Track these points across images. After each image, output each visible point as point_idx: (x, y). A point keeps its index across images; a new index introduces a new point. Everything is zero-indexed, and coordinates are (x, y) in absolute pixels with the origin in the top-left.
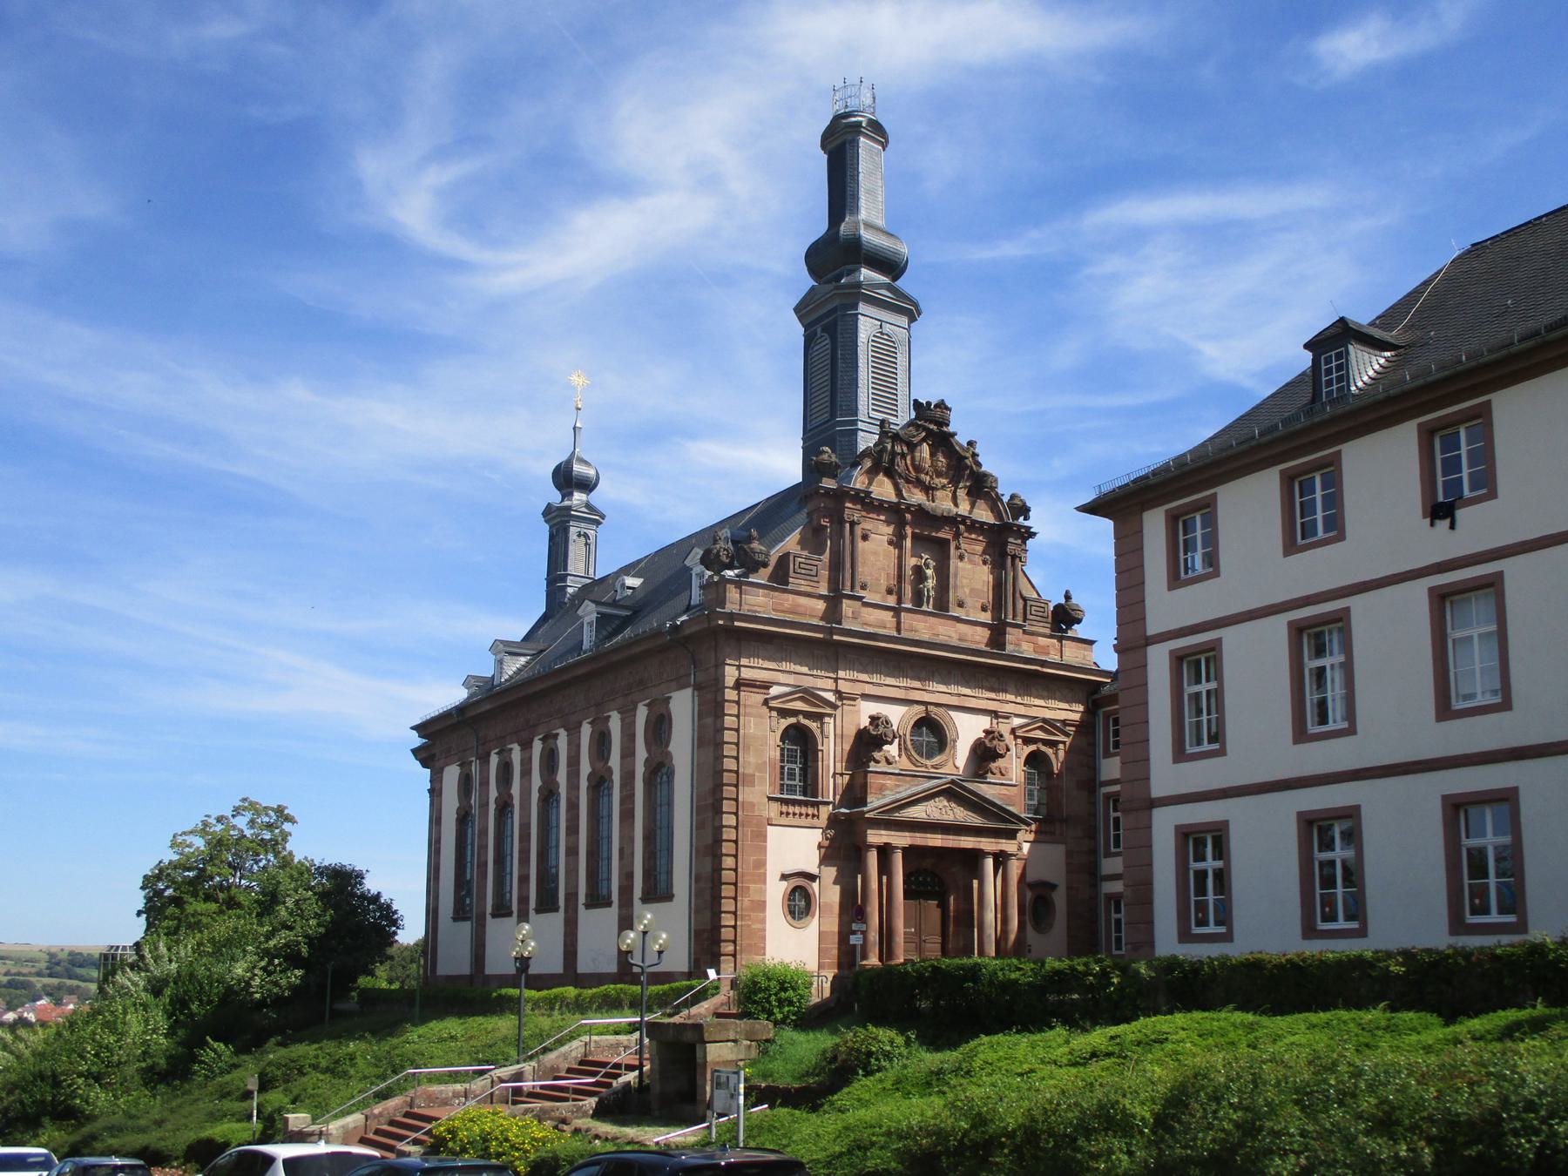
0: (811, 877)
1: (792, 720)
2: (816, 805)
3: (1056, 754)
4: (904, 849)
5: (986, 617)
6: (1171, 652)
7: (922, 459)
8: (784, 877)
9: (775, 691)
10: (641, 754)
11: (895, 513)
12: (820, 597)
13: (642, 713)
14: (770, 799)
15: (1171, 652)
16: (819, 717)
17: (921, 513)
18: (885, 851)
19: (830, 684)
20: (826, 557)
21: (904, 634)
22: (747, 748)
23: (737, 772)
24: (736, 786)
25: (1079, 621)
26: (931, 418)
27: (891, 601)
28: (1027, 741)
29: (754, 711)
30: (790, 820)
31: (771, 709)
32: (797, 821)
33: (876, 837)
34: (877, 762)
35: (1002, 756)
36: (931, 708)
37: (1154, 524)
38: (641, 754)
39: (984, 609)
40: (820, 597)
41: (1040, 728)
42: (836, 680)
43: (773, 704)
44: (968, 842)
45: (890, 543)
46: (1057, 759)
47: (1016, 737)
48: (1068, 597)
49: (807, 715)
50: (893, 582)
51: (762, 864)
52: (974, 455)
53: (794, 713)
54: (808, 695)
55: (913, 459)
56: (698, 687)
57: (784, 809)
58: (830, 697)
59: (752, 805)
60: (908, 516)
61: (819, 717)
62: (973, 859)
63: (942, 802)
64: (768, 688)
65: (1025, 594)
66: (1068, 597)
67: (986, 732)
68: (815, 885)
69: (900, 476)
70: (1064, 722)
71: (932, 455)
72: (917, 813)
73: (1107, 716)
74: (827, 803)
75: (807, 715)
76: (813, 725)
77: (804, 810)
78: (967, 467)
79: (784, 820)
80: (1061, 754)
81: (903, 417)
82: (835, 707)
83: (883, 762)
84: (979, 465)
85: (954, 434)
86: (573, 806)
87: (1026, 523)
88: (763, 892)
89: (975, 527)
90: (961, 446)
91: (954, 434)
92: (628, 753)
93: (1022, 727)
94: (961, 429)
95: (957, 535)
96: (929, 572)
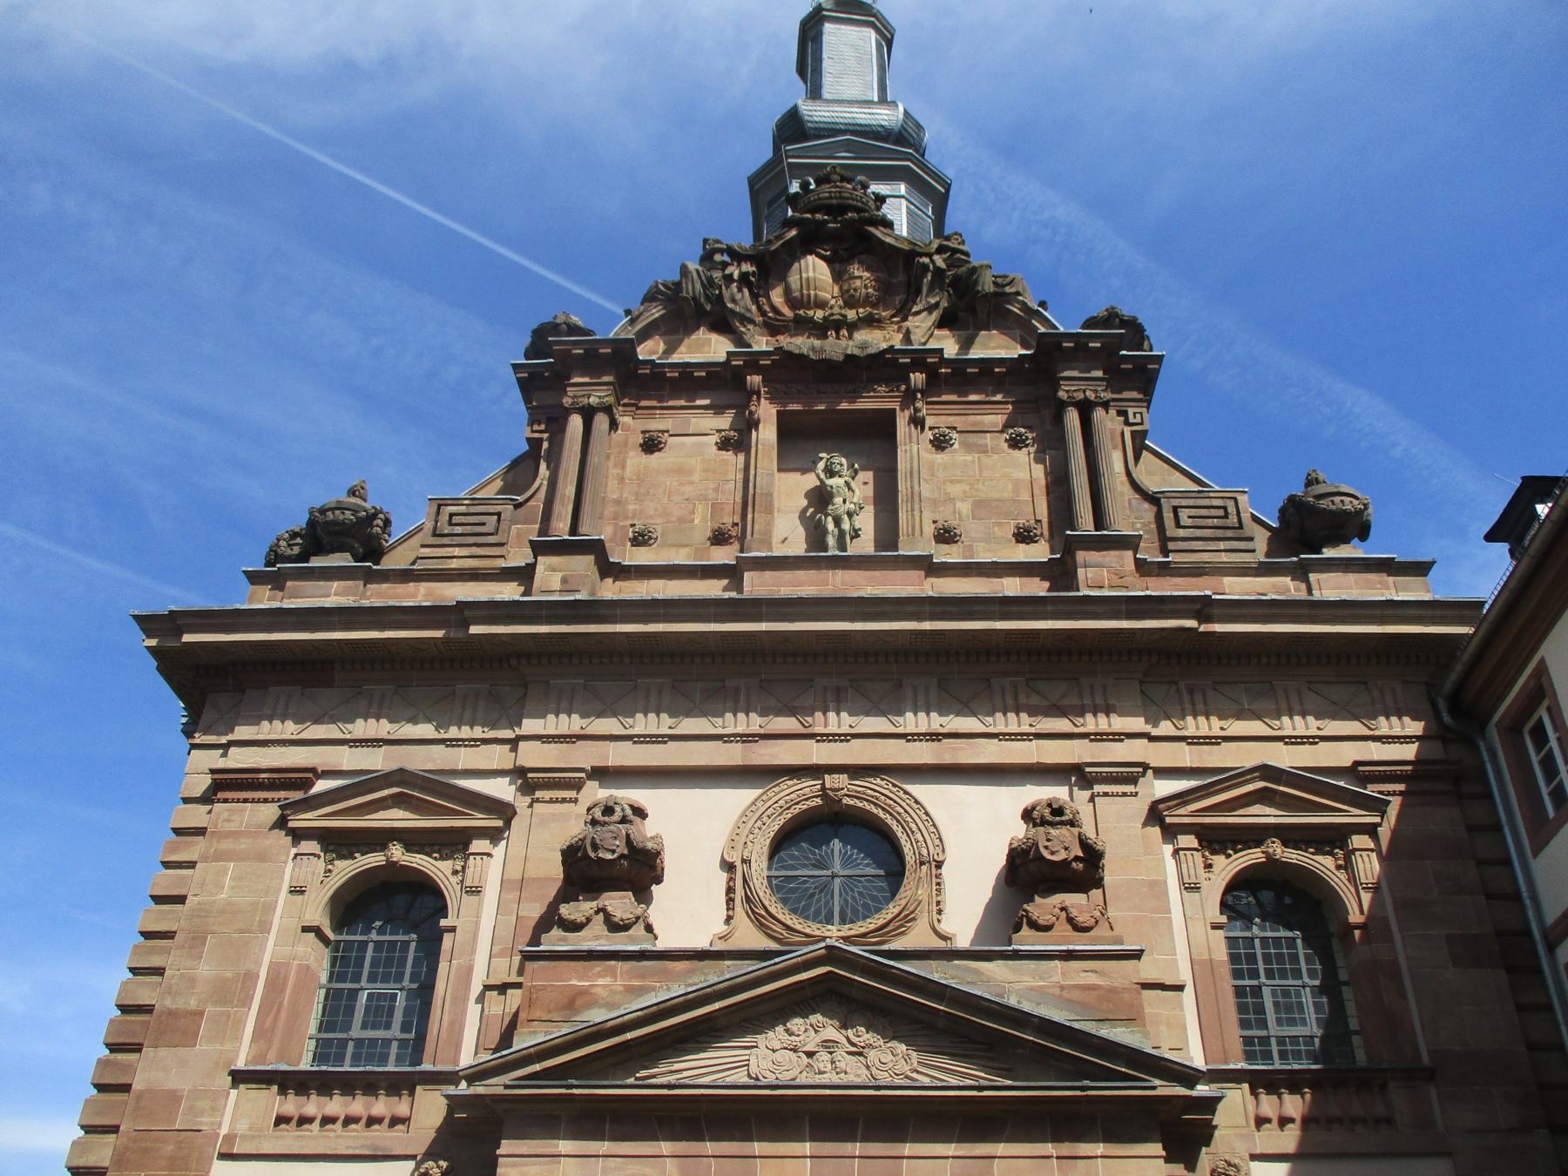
2: (401, 1085)
3: (1347, 866)
29: (244, 844)
30: (313, 1139)
31: (298, 835)
32: (337, 1139)
34: (574, 927)
36: (830, 781)
39: (1024, 536)
46: (1357, 879)
48: (1311, 482)
53: (377, 839)
58: (502, 789)
65: (1152, 486)
69: (745, 320)
70: (1355, 771)
71: (838, 277)
75: (415, 840)
76: (439, 869)
78: (925, 268)
79: (290, 1140)
80: (1369, 866)
82: (505, 811)
89: (985, 375)
93: (1182, 798)
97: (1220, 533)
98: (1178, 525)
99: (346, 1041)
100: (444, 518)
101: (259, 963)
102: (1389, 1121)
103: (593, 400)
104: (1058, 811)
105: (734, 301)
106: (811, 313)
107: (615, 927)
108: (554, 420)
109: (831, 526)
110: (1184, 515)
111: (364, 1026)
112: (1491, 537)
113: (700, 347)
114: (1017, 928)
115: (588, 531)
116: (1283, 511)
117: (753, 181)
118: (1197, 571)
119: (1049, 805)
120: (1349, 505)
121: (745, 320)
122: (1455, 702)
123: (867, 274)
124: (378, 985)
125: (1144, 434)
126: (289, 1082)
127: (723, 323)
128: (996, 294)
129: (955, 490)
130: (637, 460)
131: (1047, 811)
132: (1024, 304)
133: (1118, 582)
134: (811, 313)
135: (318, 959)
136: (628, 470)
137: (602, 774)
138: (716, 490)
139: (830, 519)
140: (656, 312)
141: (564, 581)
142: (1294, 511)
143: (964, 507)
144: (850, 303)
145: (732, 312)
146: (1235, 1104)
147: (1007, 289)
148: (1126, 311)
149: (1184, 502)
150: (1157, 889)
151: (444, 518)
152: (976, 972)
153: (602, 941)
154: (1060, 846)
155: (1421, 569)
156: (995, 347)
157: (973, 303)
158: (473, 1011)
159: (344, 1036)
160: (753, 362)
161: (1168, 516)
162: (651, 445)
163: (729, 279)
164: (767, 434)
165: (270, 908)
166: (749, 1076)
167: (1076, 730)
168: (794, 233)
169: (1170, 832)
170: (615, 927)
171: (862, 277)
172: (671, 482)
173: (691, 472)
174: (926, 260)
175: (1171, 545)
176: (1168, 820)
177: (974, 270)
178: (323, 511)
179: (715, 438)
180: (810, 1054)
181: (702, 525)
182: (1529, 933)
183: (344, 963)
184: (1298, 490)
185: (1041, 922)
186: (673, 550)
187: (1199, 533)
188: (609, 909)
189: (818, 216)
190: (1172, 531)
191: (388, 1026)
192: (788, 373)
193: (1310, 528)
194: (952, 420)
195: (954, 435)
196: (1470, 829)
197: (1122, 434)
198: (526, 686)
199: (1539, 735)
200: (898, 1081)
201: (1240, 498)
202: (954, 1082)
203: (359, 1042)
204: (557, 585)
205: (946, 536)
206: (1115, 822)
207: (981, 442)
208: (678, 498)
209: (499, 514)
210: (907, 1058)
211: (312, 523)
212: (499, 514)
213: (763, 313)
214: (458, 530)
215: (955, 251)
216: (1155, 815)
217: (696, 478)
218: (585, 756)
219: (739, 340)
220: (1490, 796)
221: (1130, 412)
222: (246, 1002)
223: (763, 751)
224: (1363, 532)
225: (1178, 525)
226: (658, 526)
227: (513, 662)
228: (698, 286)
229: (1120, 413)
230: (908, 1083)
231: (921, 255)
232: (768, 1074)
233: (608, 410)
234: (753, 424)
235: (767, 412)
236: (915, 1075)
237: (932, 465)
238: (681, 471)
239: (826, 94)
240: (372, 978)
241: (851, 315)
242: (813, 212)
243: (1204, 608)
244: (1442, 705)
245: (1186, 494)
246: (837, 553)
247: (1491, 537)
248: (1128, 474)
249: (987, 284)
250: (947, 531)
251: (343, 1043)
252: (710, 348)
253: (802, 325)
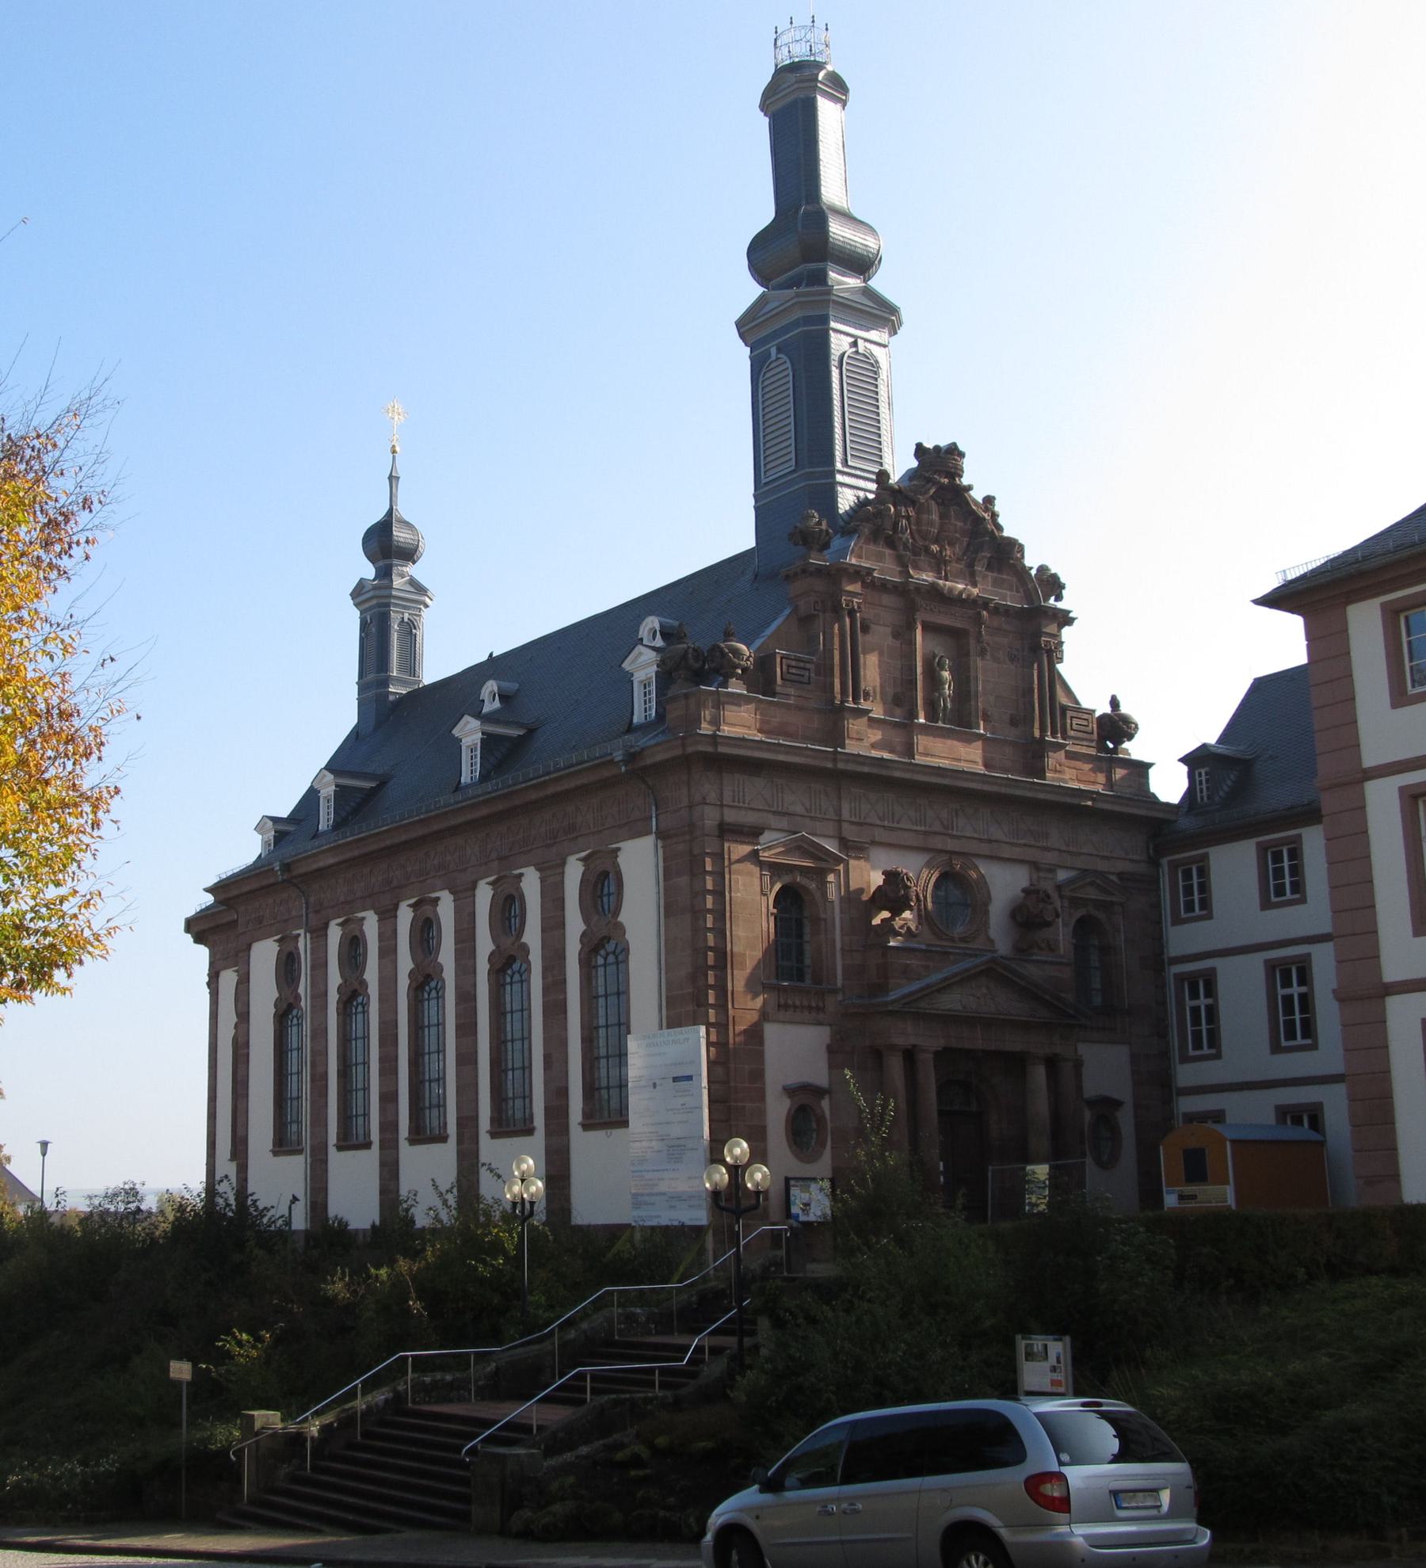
0: (818, 1092)
1: (787, 879)
4: (937, 1053)
6: (1402, 790)
7: (931, 523)
8: (790, 1091)
9: (766, 837)
10: (575, 925)
13: (574, 872)
15: (1402, 790)
16: (820, 874)
17: (935, 594)
18: (910, 1056)
21: (919, 759)
25: (1130, 737)
26: (939, 465)
31: (761, 865)
33: (905, 1034)
35: (1048, 924)
37: (1365, 622)
38: (575, 925)
41: (1092, 883)
43: (765, 856)
44: (1013, 1043)
47: (1061, 897)
48: (1114, 703)
51: (758, 1075)
52: (994, 516)
53: (791, 869)
55: (919, 522)
56: (661, 835)
58: (831, 846)
62: (1016, 1063)
66: (1114, 703)
67: (1024, 890)
68: (825, 1104)
71: (941, 517)
72: (952, 1001)
73: (1174, 867)
74: (835, 991)
81: (900, 463)
82: (839, 860)
84: (1000, 528)
85: (970, 488)
86: (466, 998)
87: (1060, 605)
88: (762, 1113)
90: (974, 501)
91: (970, 488)
92: (553, 925)
94: (978, 479)
96: (946, 674)
110: (1075, 721)
112: (1181, 760)
121: (906, 548)
164: (919, 631)
199: (1188, 875)
234: (911, 628)
247: (1181, 760)
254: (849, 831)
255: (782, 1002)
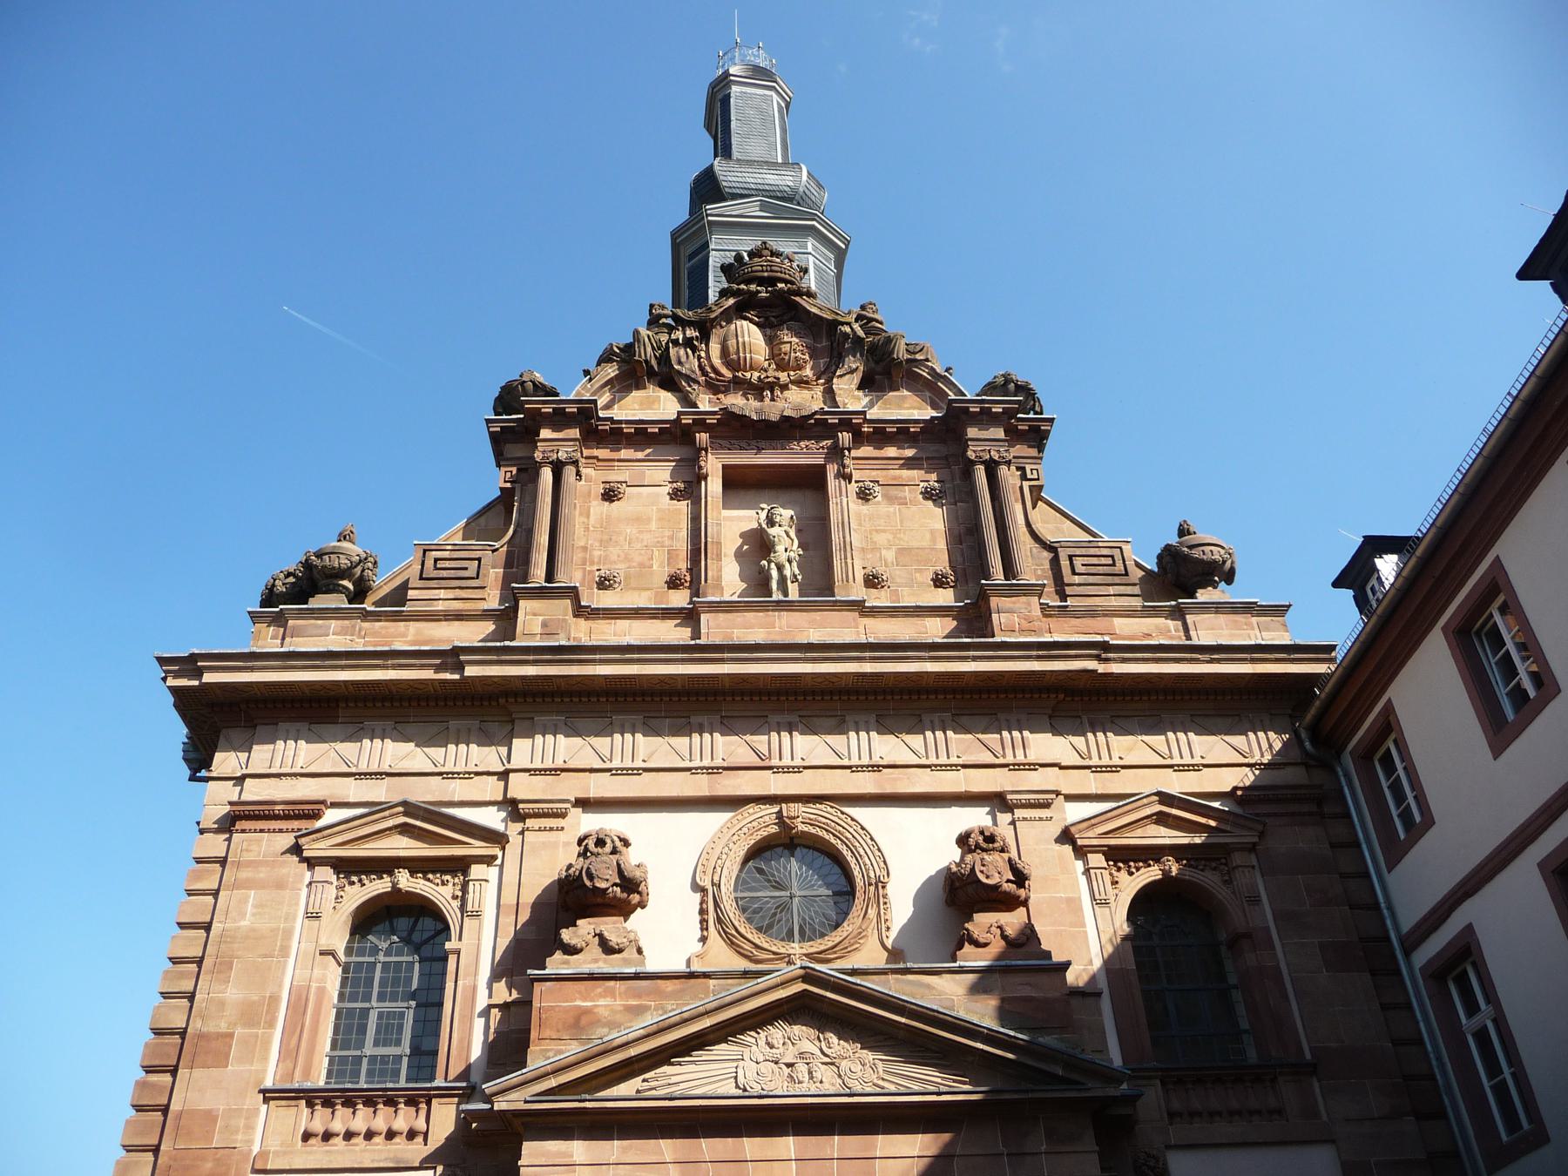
1: (381, 886)
5: (946, 597)
9: (331, 816)
11: (675, 438)
12: (485, 615)
14: (268, 1095)
19: (491, 789)
20: (502, 544)
22: (224, 966)
23: (183, 1033)
24: (174, 1072)
27: (680, 599)
28: (1122, 856)
31: (312, 863)
34: (571, 950)
39: (939, 582)
40: (485, 615)
42: (504, 775)
43: (314, 849)
45: (675, 495)
48: (1183, 531)
49: (418, 866)
50: (683, 565)
53: (384, 866)
54: (424, 818)
57: (320, 1119)
58: (492, 818)
59: (210, 1117)
60: (703, 438)
61: (459, 866)
63: (800, 1039)
64: (316, 816)
65: (1050, 537)
71: (771, 341)
75: (418, 866)
76: (440, 892)
77: (381, 1121)
82: (498, 839)
83: (595, 950)
89: (899, 433)
95: (836, 453)
97: (1109, 579)
98: (1074, 573)
99: (360, 1058)
100: (429, 563)
101: (280, 986)
102: (1279, 1112)
103: (562, 456)
104: (990, 839)
105: (680, 363)
106: (748, 375)
107: (607, 948)
108: (527, 473)
109: (774, 573)
110: (1078, 562)
111: (376, 1044)
112: (1337, 584)
113: (650, 403)
114: (960, 947)
115: (562, 580)
116: (1160, 557)
117: (675, 235)
118: (1092, 613)
119: (982, 833)
120: (1217, 555)
122: (1314, 730)
123: (795, 340)
124: (387, 1004)
125: (1040, 488)
126: (310, 1097)
127: (669, 380)
128: (908, 361)
129: (881, 539)
130: (599, 508)
131: (981, 838)
132: (933, 369)
133: (1025, 625)
134: (748, 375)
135: (332, 978)
136: (592, 520)
137: (585, 804)
138: (671, 538)
139: (773, 565)
140: (611, 371)
141: (544, 625)
142: (1169, 555)
143: (890, 555)
144: (782, 366)
145: (679, 372)
146: (1152, 1099)
147: (919, 357)
148: (1021, 377)
149: (1078, 552)
150: (1073, 904)
151: (429, 563)
152: (929, 986)
153: (601, 964)
154: (994, 871)
155: (1280, 610)
156: (908, 407)
157: (886, 368)
158: (479, 1024)
159: (358, 1053)
160: (700, 424)
161: (1065, 563)
162: (610, 495)
163: (676, 343)
164: (714, 486)
165: (288, 934)
166: (737, 1087)
167: (997, 761)
168: (731, 301)
169: (1081, 852)
170: (607, 948)
171: (792, 342)
172: (630, 530)
173: (649, 520)
174: (848, 329)
175: (1068, 590)
176: (1080, 842)
177: (889, 340)
178: (319, 555)
179: (668, 489)
180: (789, 1065)
181: (661, 572)
182: (1388, 939)
183: (355, 981)
184: (1173, 540)
185: (982, 940)
186: (636, 593)
187: (1091, 579)
188: (606, 934)
189: (753, 287)
190: (1067, 577)
191: (398, 1043)
192: (734, 429)
193: (1182, 574)
194: (874, 474)
195: (877, 488)
196: (1332, 846)
197: (1021, 488)
198: (513, 722)
199: (1387, 761)
200: (868, 1090)
201: (1124, 547)
202: (916, 1087)
203: (373, 1059)
204: (538, 630)
205: (872, 581)
206: (1034, 841)
207: (901, 495)
208: (639, 546)
209: (479, 560)
210: (874, 1068)
211: (307, 565)
212: (479, 560)
213: (704, 373)
214: (445, 574)
215: (871, 320)
216: (1066, 837)
217: (653, 526)
218: (571, 787)
219: (686, 401)
220: (1349, 816)
221: (1028, 468)
222: (271, 1024)
223: (726, 782)
224: (1229, 577)
225: (1074, 573)
226: (620, 569)
227: (502, 701)
228: (649, 349)
229: (1018, 469)
230: (878, 1090)
231: (843, 324)
232: (755, 1085)
233: (575, 463)
235: (713, 466)
236: (881, 1083)
237: (859, 515)
238: (638, 520)
239: (735, 155)
240: (381, 998)
241: (783, 377)
242: (748, 282)
243: (1103, 649)
244: (1303, 735)
245: (1078, 545)
246: (781, 598)
247: (1337, 584)
248: (1028, 524)
249: (901, 353)
250: (875, 577)
251: (358, 1060)
252: (660, 406)
253: (739, 385)
254: (521, 787)
255: (318, 1126)
